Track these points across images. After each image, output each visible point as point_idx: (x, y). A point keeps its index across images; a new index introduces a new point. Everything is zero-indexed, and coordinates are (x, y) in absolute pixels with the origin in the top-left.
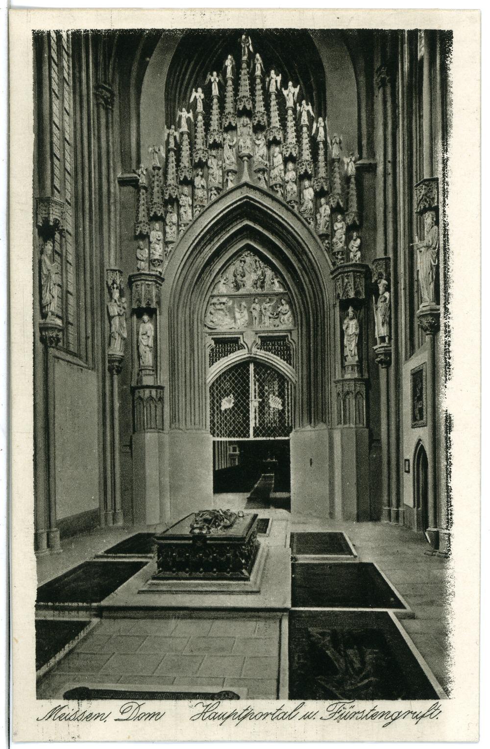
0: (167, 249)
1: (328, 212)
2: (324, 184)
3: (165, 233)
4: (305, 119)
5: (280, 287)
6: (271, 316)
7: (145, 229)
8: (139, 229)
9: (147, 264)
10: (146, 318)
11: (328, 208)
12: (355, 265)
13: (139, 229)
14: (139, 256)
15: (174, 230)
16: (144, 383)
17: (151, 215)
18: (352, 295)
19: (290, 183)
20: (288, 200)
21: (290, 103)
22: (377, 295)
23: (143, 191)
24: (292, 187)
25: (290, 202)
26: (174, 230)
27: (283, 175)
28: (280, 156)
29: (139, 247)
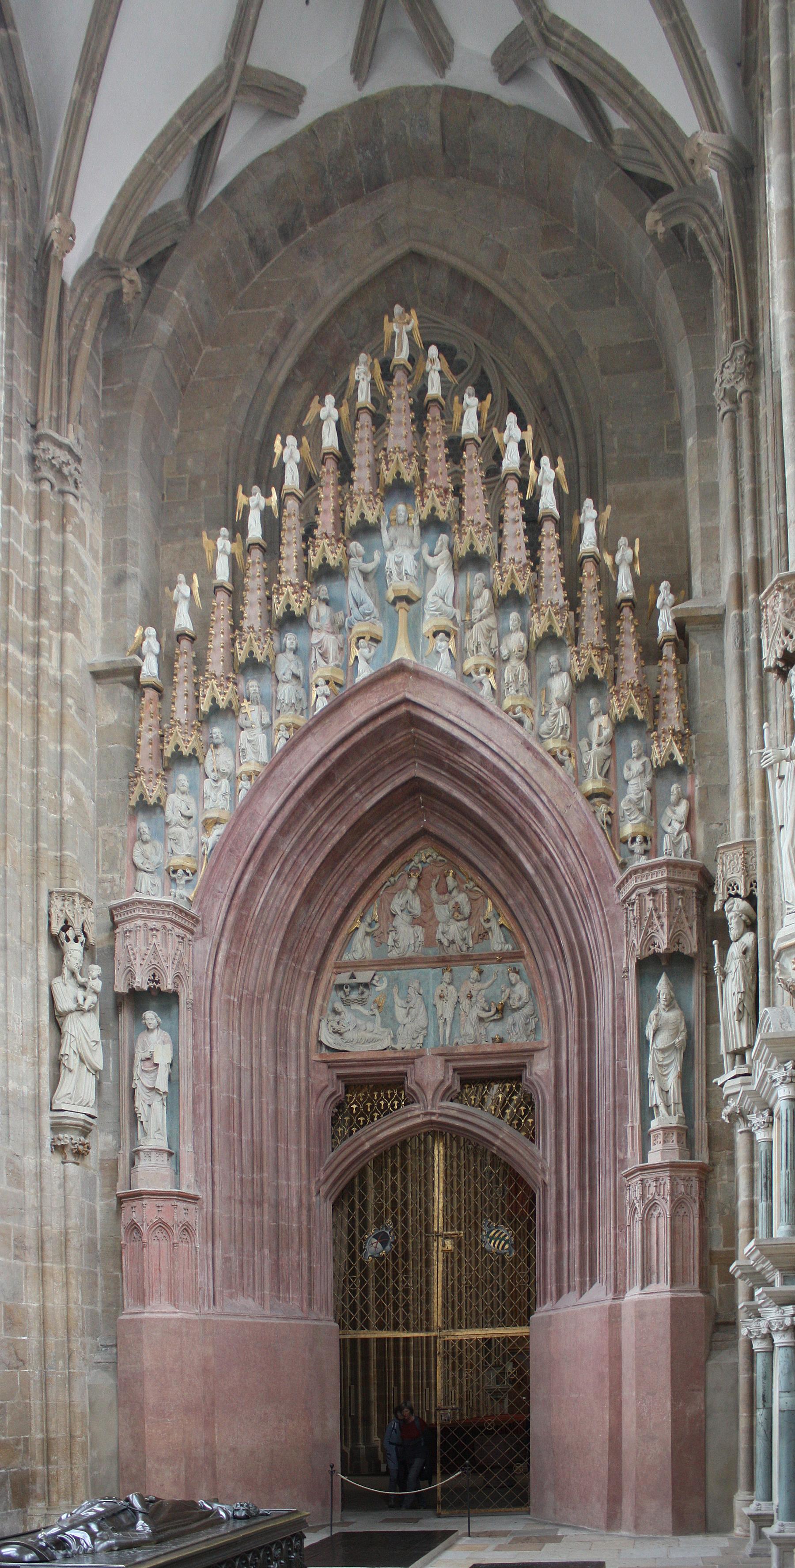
0: (204, 838)
1: (607, 732)
2: (595, 660)
3: (201, 798)
4: (548, 502)
5: (507, 942)
6: (484, 1015)
7: (152, 790)
8: (137, 790)
9: (158, 881)
10: (150, 1016)
11: (603, 720)
12: (668, 864)
13: (137, 790)
14: (138, 861)
15: (223, 789)
16: (142, 1187)
17: (168, 754)
18: (662, 942)
19: (513, 662)
20: (507, 703)
21: (511, 460)
22: (726, 944)
23: (150, 693)
24: (515, 669)
25: (511, 710)
26: (223, 789)
27: (494, 640)
28: (486, 593)
29: (139, 838)
